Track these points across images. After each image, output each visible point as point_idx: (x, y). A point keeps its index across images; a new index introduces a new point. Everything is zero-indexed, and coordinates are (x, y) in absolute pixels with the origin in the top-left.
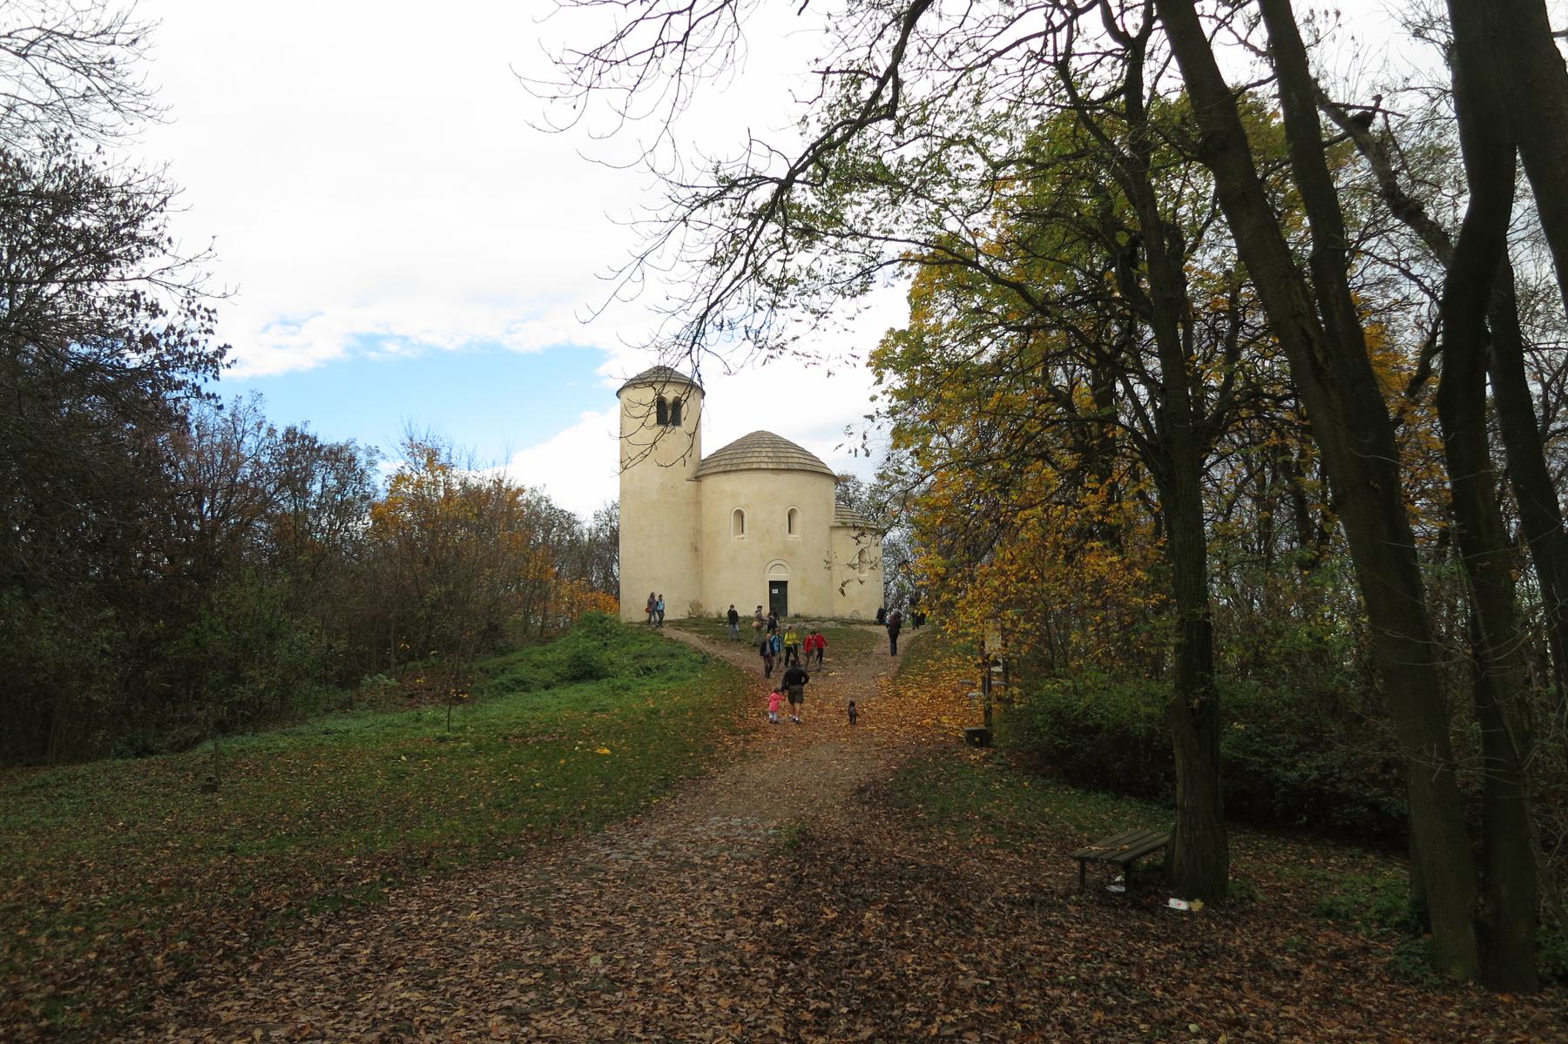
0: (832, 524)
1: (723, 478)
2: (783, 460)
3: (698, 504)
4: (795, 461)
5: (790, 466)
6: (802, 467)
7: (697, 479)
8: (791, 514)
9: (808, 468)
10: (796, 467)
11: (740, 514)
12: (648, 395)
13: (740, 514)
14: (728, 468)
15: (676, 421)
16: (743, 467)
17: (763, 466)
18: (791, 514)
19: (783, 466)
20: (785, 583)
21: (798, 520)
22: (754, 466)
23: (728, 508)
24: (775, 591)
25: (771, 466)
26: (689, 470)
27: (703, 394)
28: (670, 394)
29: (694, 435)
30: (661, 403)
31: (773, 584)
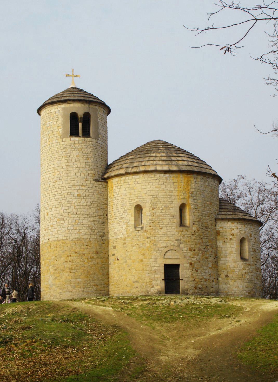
4: (184, 163)
9: (195, 169)
14: (130, 170)
17: (159, 168)
19: (175, 168)
20: (177, 267)
27: (109, 111)
30: (73, 117)
31: (167, 267)
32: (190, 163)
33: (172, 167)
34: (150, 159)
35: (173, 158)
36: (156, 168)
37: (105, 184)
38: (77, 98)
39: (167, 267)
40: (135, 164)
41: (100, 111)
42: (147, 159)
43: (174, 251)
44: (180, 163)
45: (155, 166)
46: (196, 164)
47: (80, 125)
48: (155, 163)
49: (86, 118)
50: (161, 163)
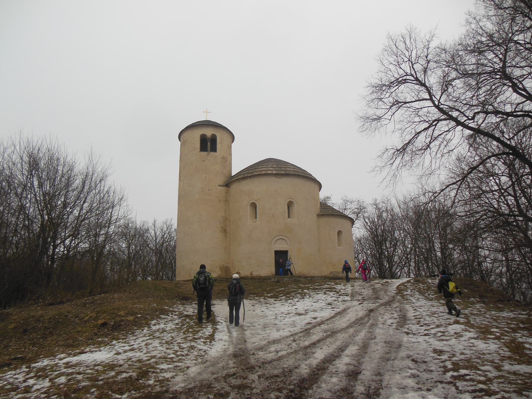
1: (243, 183)
2: (282, 169)
3: (227, 201)
5: (288, 172)
7: (227, 185)
8: (290, 205)
10: (292, 173)
11: (254, 206)
12: (197, 134)
13: (254, 206)
14: (246, 175)
15: (214, 149)
16: (256, 173)
17: (269, 172)
18: (290, 205)
19: (283, 172)
20: (285, 253)
22: (263, 172)
25: (274, 172)
26: (221, 180)
28: (209, 132)
29: (227, 161)
31: (277, 253)
32: (295, 170)
37: (228, 188)
39: (277, 253)
40: (250, 171)
41: (226, 137)
42: (261, 167)
43: (284, 241)
44: (288, 169)
46: (300, 171)
47: (209, 144)
48: (267, 169)
49: (214, 139)
50: (271, 169)
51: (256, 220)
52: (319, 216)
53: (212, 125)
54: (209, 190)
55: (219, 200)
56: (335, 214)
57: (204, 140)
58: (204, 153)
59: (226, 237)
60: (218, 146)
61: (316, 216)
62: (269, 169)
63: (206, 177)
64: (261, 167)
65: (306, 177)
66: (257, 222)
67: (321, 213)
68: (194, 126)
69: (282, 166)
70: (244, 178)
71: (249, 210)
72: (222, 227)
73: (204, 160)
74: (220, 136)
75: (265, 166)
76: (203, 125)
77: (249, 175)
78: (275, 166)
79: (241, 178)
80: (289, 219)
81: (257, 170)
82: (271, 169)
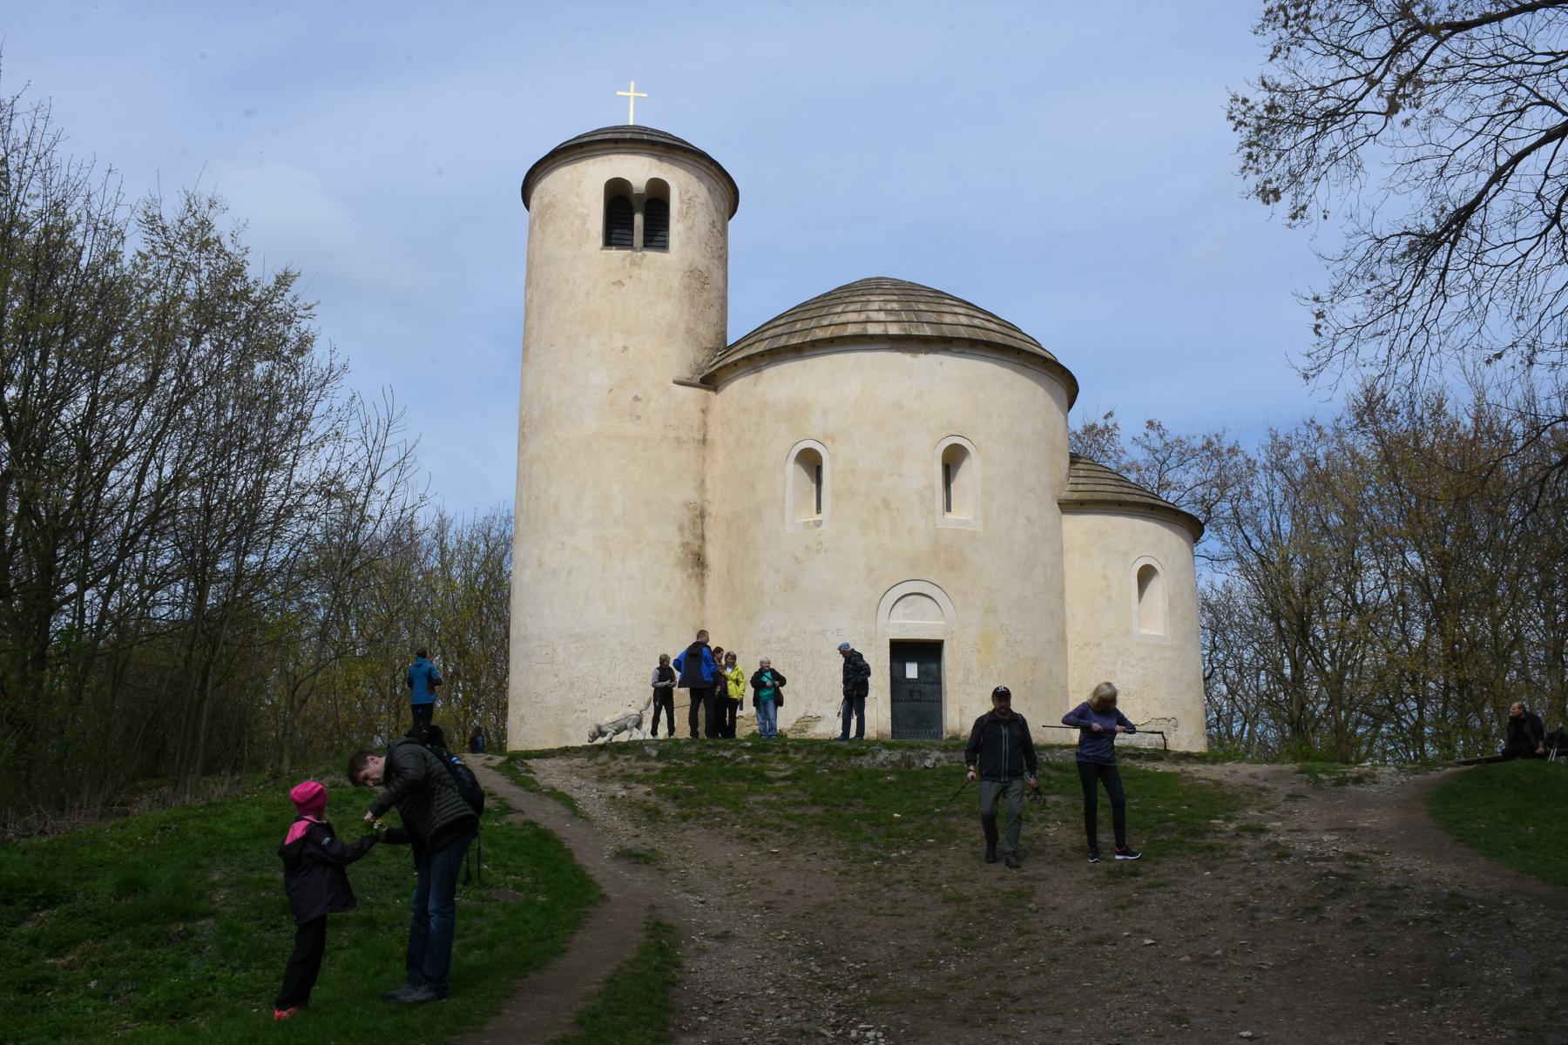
0: (1065, 495)
2: (926, 317)
4: (956, 322)
5: (947, 331)
6: (981, 335)
8: (953, 459)
10: (964, 333)
11: (811, 462)
13: (811, 462)
14: (782, 341)
16: (820, 334)
17: (873, 329)
18: (953, 459)
19: (927, 331)
21: (967, 475)
22: (851, 330)
23: (783, 448)
24: (912, 671)
25: (894, 330)
28: (638, 170)
32: (977, 322)
33: (917, 327)
34: (847, 310)
35: (922, 307)
36: (865, 329)
37: (711, 394)
38: (628, 136)
40: (799, 326)
42: (839, 309)
44: (948, 319)
45: (862, 326)
46: (992, 326)
47: (639, 219)
48: (863, 317)
49: (656, 202)
50: (882, 316)
51: (818, 517)
52: (1071, 506)
53: (654, 143)
54: (637, 399)
55: (678, 440)
56: (1128, 498)
57: (618, 199)
58: (616, 254)
59: (703, 585)
60: (676, 227)
61: (1057, 506)
62: (874, 316)
63: (625, 348)
64: (839, 309)
65: (1019, 351)
66: (823, 527)
67: (1075, 496)
68: (581, 145)
69: (922, 307)
70: (776, 355)
71: (791, 480)
72: (685, 545)
73: (620, 283)
74: (681, 183)
75: (857, 307)
76: (616, 141)
77: (794, 341)
78: (895, 306)
79: (761, 354)
80: (948, 515)
81: (825, 322)
82: (882, 316)
